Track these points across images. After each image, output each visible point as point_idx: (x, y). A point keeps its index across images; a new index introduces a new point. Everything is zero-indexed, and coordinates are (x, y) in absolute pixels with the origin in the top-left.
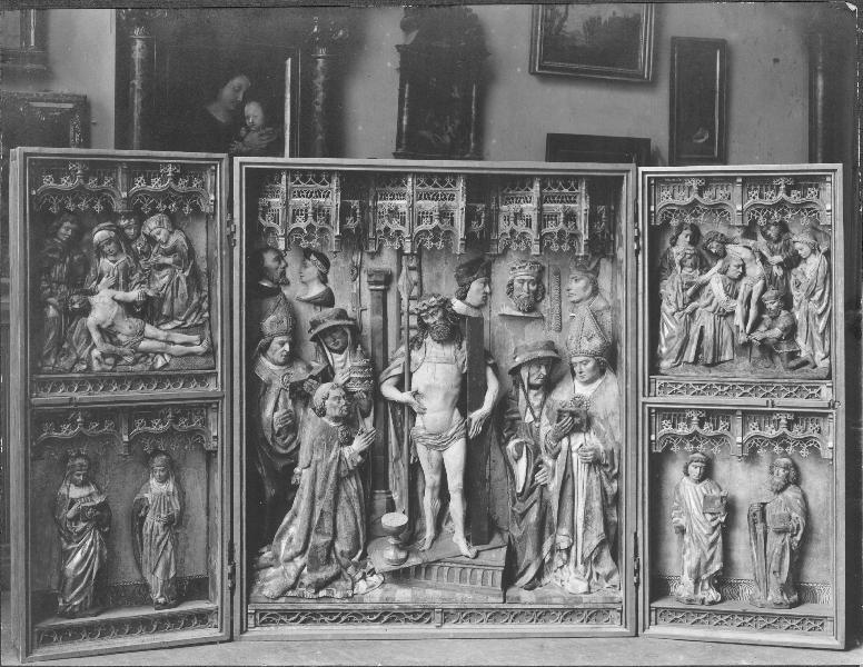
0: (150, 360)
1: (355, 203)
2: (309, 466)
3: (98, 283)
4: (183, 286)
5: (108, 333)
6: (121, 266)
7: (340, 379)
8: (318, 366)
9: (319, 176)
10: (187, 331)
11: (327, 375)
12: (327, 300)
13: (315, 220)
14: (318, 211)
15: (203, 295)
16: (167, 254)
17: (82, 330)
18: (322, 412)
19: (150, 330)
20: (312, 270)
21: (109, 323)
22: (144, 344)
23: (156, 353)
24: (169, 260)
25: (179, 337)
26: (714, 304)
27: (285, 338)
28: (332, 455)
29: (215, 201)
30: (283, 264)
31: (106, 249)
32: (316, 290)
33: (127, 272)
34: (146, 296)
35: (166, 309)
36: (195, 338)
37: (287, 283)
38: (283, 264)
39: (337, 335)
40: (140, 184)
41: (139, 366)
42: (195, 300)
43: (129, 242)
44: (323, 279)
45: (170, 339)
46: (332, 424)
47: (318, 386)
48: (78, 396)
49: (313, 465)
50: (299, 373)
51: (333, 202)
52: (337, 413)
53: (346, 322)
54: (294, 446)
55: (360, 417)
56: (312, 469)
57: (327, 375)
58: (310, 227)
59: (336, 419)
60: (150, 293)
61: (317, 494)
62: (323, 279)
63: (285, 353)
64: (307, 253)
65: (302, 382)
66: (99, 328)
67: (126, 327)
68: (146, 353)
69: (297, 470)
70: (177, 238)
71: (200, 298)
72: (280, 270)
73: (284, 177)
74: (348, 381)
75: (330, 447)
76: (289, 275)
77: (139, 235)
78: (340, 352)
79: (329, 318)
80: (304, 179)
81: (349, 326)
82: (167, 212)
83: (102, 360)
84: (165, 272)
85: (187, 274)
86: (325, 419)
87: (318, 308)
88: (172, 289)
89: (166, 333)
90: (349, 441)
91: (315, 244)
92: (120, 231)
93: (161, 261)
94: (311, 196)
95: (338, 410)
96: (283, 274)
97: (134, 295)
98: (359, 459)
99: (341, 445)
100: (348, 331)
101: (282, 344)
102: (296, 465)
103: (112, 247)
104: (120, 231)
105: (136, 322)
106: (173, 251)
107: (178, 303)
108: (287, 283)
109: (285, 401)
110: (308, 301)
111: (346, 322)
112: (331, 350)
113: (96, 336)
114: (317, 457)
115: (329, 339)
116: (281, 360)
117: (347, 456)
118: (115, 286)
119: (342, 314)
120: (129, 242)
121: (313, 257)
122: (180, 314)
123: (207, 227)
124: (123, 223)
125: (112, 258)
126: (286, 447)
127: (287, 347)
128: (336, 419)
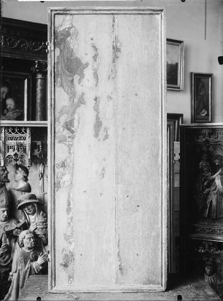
1: (39, 143)
2: (16, 272)
7: (32, 228)
8: (22, 221)
9: (20, 129)
11: (26, 226)
12: (28, 189)
13: (18, 151)
14: (21, 147)
18: (22, 245)
20: (20, 174)
26: (217, 190)
27: (4, 209)
28: (27, 266)
30: (6, 172)
32: (22, 184)
37: (9, 181)
38: (6, 172)
39: (30, 207)
44: (26, 179)
46: (28, 251)
47: (20, 232)
49: (18, 272)
50: (13, 225)
51: (27, 142)
52: (29, 246)
53: (34, 201)
54: (9, 261)
55: (43, 246)
56: (17, 274)
57: (26, 226)
58: (16, 155)
59: (29, 249)
61: (20, 286)
62: (26, 179)
63: (5, 216)
64: (17, 167)
65: (12, 231)
69: (11, 273)
72: (4, 176)
73: (3, 130)
74: (36, 229)
75: (25, 263)
76: (9, 178)
78: (33, 214)
79: (26, 199)
80: (13, 131)
81: (35, 202)
86: (23, 248)
87: (23, 193)
90: (36, 259)
91: (19, 163)
94: (17, 140)
95: (29, 244)
96: (6, 177)
98: (41, 268)
99: (32, 261)
100: (35, 205)
101: (4, 211)
102: (10, 271)
108: (9, 181)
109: (5, 240)
110: (18, 190)
111: (34, 201)
112: (28, 214)
114: (19, 268)
115: (26, 209)
116: (3, 219)
117: (34, 267)
119: (33, 197)
121: (20, 169)
126: (5, 262)
127: (6, 213)
128: (29, 249)
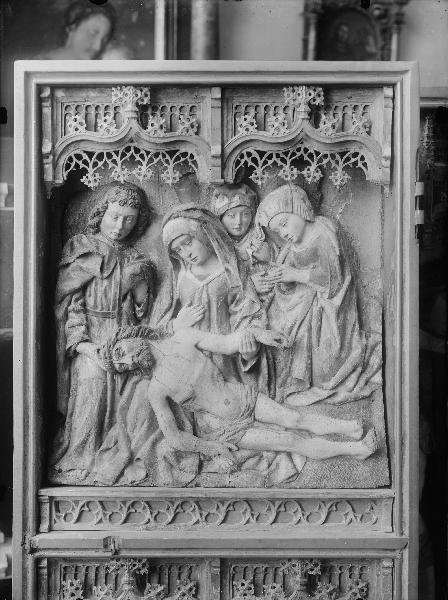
0: (264, 464)
3: (174, 316)
4: (331, 326)
5: (183, 413)
6: (213, 288)
10: (338, 410)
15: (371, 342)
16: (300, 263)
17: (140, 406)
19: (265, 407)
21: (185, 395)
22: (252, 437)
23: (277, 453)
24: (303, 275)
25: (320, 423)
29: (392, 158)
31: (183, 254)
33: (227, 302)
34: (259, 345)
35: (299, 368)
36: (352, 426)
40: (245, 128)
41: (243, 477)
42: (356, 353)
43: (231, 240)
45: (303, 426)
48: (122, 532)
60: (266, 338)
66: (170, 402)
67: (220, 402)
68: (257, 453)
70: (322, 233)
71: (365, 350)
77: (251, 226)
82: (300, 182)
83: (172, 459)
84: (295, 297)
85: (338, 300)
88: (310, 329)
89: (296, 415)
92: (208, 218)
93: (287, 278)
97: (236, 341)
103: (195, 249)
104: (208, 218)
105: (239, 391)
106: (314, 255)
107: (323, 357)
113: (164, 417)
118: (204, 321)
120: (231, 240)
122: (325, 378)
123: (382, 214)
124: (219, 204)
125: (198, 270)
